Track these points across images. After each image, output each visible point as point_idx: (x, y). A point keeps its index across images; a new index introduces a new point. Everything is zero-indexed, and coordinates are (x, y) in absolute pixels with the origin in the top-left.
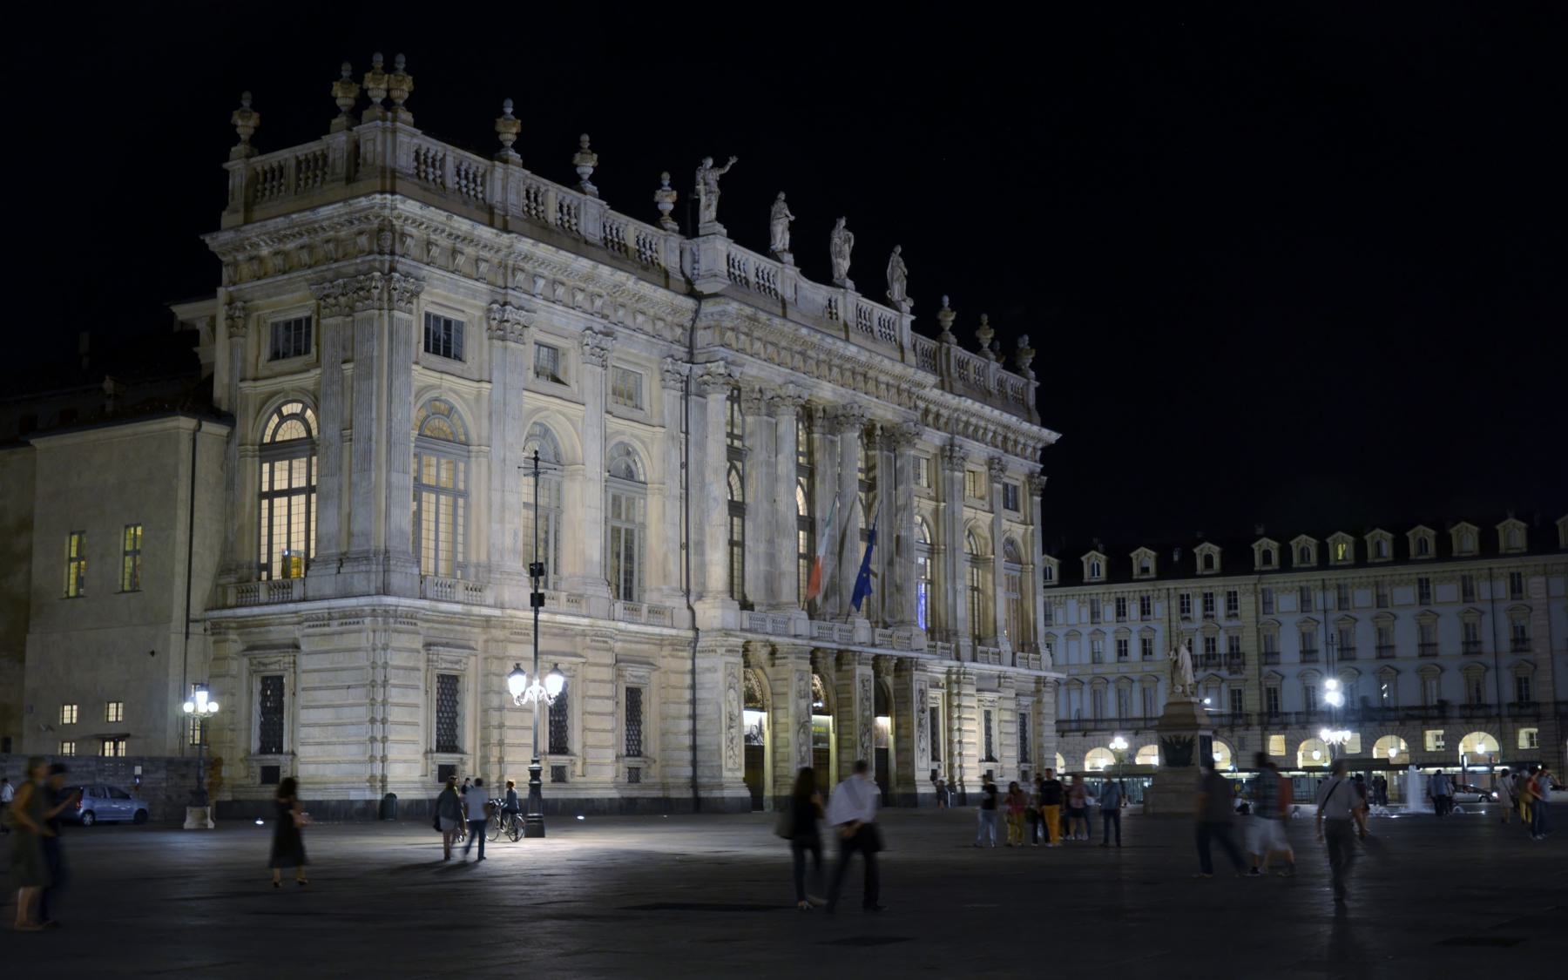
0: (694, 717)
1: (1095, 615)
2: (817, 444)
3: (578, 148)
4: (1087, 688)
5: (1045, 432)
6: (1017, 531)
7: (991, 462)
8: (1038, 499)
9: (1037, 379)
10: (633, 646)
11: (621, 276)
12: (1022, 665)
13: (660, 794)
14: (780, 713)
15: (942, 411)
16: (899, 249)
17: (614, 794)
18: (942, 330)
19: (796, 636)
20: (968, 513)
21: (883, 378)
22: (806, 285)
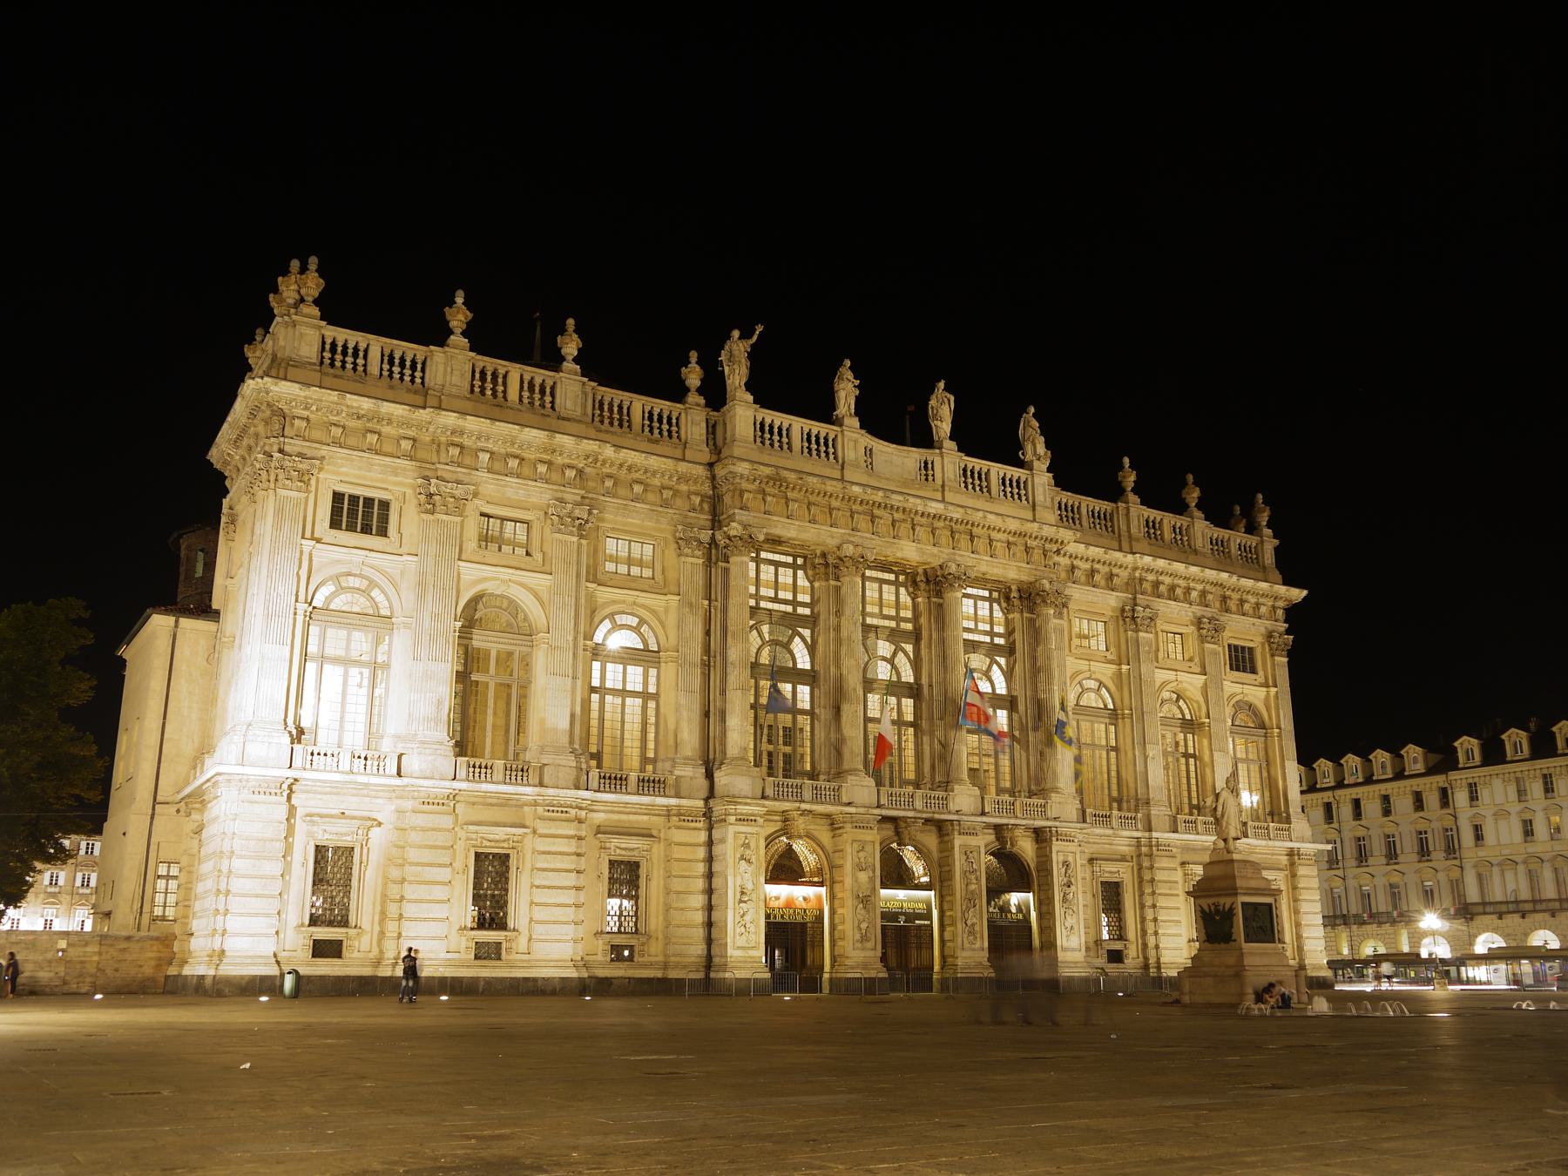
0: (709, 891)
1: (1521, 793)
2: (922, 607)
3: (563, 331)
4: (1521, 868)
6: (1256, 694)
7: (1198, 623)
9: (1275, 537)
10: (624, 817)
11: (590, 446)
12: (1256, 836)
13: (659, 974)
14: (837, 887)
15: (1115, 571)
16: (1032, 410)
18: (1188, 506)
20: (1161, 676)
21: (994, 535)
22: (883, 448)
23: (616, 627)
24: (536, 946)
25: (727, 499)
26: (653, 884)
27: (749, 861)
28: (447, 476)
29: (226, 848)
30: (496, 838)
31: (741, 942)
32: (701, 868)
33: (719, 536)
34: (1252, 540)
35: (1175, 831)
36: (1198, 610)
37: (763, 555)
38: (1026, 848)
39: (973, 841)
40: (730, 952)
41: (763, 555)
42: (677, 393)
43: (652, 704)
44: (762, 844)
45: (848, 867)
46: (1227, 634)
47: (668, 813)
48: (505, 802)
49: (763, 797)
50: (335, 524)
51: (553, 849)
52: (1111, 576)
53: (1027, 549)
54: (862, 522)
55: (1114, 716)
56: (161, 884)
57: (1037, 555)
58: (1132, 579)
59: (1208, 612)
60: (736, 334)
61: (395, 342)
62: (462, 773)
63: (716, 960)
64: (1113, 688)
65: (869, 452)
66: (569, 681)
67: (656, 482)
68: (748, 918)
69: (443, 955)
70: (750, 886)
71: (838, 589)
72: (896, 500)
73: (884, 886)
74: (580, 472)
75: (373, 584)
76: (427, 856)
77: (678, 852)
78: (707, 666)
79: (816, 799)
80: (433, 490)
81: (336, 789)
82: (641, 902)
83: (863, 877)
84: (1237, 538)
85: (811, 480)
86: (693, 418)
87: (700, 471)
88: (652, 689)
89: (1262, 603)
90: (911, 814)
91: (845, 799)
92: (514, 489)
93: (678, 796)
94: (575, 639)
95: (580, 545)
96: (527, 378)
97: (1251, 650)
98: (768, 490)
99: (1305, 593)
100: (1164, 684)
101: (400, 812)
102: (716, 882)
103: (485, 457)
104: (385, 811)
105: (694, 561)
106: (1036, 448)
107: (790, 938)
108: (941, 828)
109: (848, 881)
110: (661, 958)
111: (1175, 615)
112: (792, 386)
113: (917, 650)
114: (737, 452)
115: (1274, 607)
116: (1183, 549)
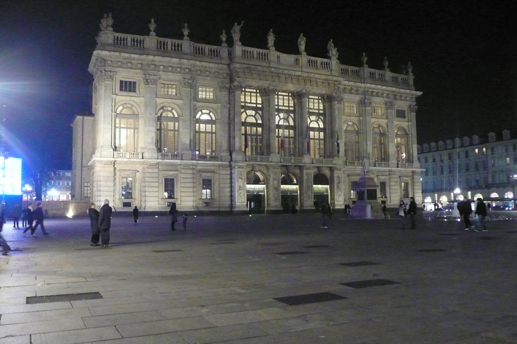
0: (231, 187)
3: (184, 27)
5: (414, 92)
7: (386, 103)
8: (415, 114)
9: (413, 75)
12: (402, 167)
13: (218, 210)
14: (269, 185)
15: (359, 89)
17: (193, 210)
19: (271, 162)
20: (373, 120)
21: (318, 80)
23: (202, 114)
24: (182, 203)
25: (234, 74)
26: (216, 186)
27: (242, 179)
28: (151, 74)
29: (99, 179)
30: (171, 174)
31: (240, 201)
32: (229, 181)
33: (232, 86)
34: (406, 77)
35: (375, 166)
36: (386, 100)
37: (247, 90)
38: (327, 172)
39: (309, 171)
40: (236, 203)
41: (247, 90)
42: (218, 43)
43: (214, 135)
44: (245, 173)
45: (271, 179)
46: (395, 106)
47: (219, 166)
48: (172, 165)
49: (246, 161)
50: (121, 90)
51: (187, 177)
52: (357, 90)
53: (329, 84)
54: (276, 79)
55: (358, 133)
56: (86, 188)
57: (332, 85)
58: (365, 91)
59: (389, 100)
60: (236, 24)
61: (135, 36)
62: (160, 157)
63: (234, 206)
64: (358, 124)
65: (278, 57)
66: (189, 130)
67: (213, 71)
68: (242, 194)
69: (157, 206)
70: (242, 185)
71: (269, 99)
72: (286, 72)
73: (282, 184)
74: (190, 70)
75: (133, 106)
76: (151, 180)
77: (222, 177)
78: (229, 124)
79: (261, 161)
80: (147, 78)
81: (126, 163)
82: (212, 190)
83: (276, 182)
84: (400, 77)
85: (259, 67)
86: (224, 51)
87: (225, 67)
88: (214, 131)
89: (408, 96)
90: (290, 164)
91: (270, 160)
92: (171, 76)
93: (221, 161)
94: (190, 118)
95: (191, 91)
96: (173, 43)
97: (404, 111)
98: (246, 71)
99: (422, 93)
100: (373, 123)
101: (144, 168)
102: (233, 184)
103: (162, 67)
104: (139, 168)
105: (225, 93)
106: (334, 52)
107: (255, 198)
108: (301, 168)
109: (271, 183)
110: (218, 205)
111: (378, 102)
112: (254, 39)
113: (294, 115)
114: (237, 60)
115: (412, 98)
116: (382, 81)
